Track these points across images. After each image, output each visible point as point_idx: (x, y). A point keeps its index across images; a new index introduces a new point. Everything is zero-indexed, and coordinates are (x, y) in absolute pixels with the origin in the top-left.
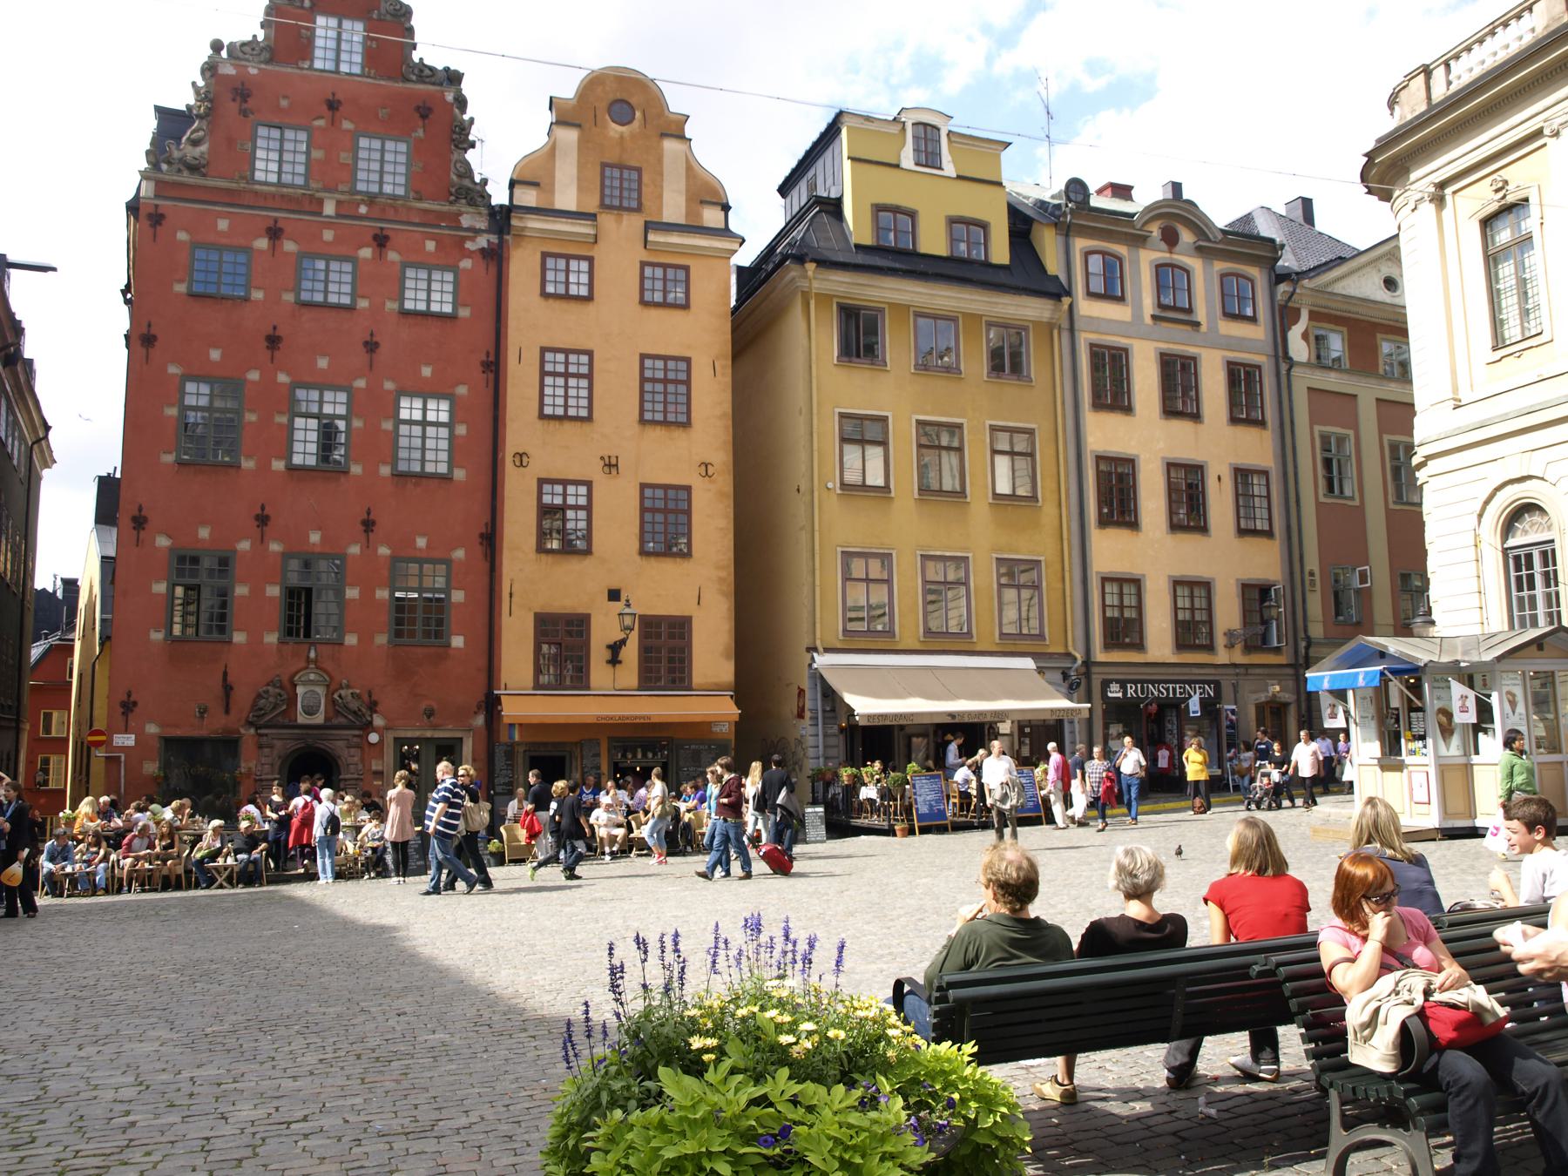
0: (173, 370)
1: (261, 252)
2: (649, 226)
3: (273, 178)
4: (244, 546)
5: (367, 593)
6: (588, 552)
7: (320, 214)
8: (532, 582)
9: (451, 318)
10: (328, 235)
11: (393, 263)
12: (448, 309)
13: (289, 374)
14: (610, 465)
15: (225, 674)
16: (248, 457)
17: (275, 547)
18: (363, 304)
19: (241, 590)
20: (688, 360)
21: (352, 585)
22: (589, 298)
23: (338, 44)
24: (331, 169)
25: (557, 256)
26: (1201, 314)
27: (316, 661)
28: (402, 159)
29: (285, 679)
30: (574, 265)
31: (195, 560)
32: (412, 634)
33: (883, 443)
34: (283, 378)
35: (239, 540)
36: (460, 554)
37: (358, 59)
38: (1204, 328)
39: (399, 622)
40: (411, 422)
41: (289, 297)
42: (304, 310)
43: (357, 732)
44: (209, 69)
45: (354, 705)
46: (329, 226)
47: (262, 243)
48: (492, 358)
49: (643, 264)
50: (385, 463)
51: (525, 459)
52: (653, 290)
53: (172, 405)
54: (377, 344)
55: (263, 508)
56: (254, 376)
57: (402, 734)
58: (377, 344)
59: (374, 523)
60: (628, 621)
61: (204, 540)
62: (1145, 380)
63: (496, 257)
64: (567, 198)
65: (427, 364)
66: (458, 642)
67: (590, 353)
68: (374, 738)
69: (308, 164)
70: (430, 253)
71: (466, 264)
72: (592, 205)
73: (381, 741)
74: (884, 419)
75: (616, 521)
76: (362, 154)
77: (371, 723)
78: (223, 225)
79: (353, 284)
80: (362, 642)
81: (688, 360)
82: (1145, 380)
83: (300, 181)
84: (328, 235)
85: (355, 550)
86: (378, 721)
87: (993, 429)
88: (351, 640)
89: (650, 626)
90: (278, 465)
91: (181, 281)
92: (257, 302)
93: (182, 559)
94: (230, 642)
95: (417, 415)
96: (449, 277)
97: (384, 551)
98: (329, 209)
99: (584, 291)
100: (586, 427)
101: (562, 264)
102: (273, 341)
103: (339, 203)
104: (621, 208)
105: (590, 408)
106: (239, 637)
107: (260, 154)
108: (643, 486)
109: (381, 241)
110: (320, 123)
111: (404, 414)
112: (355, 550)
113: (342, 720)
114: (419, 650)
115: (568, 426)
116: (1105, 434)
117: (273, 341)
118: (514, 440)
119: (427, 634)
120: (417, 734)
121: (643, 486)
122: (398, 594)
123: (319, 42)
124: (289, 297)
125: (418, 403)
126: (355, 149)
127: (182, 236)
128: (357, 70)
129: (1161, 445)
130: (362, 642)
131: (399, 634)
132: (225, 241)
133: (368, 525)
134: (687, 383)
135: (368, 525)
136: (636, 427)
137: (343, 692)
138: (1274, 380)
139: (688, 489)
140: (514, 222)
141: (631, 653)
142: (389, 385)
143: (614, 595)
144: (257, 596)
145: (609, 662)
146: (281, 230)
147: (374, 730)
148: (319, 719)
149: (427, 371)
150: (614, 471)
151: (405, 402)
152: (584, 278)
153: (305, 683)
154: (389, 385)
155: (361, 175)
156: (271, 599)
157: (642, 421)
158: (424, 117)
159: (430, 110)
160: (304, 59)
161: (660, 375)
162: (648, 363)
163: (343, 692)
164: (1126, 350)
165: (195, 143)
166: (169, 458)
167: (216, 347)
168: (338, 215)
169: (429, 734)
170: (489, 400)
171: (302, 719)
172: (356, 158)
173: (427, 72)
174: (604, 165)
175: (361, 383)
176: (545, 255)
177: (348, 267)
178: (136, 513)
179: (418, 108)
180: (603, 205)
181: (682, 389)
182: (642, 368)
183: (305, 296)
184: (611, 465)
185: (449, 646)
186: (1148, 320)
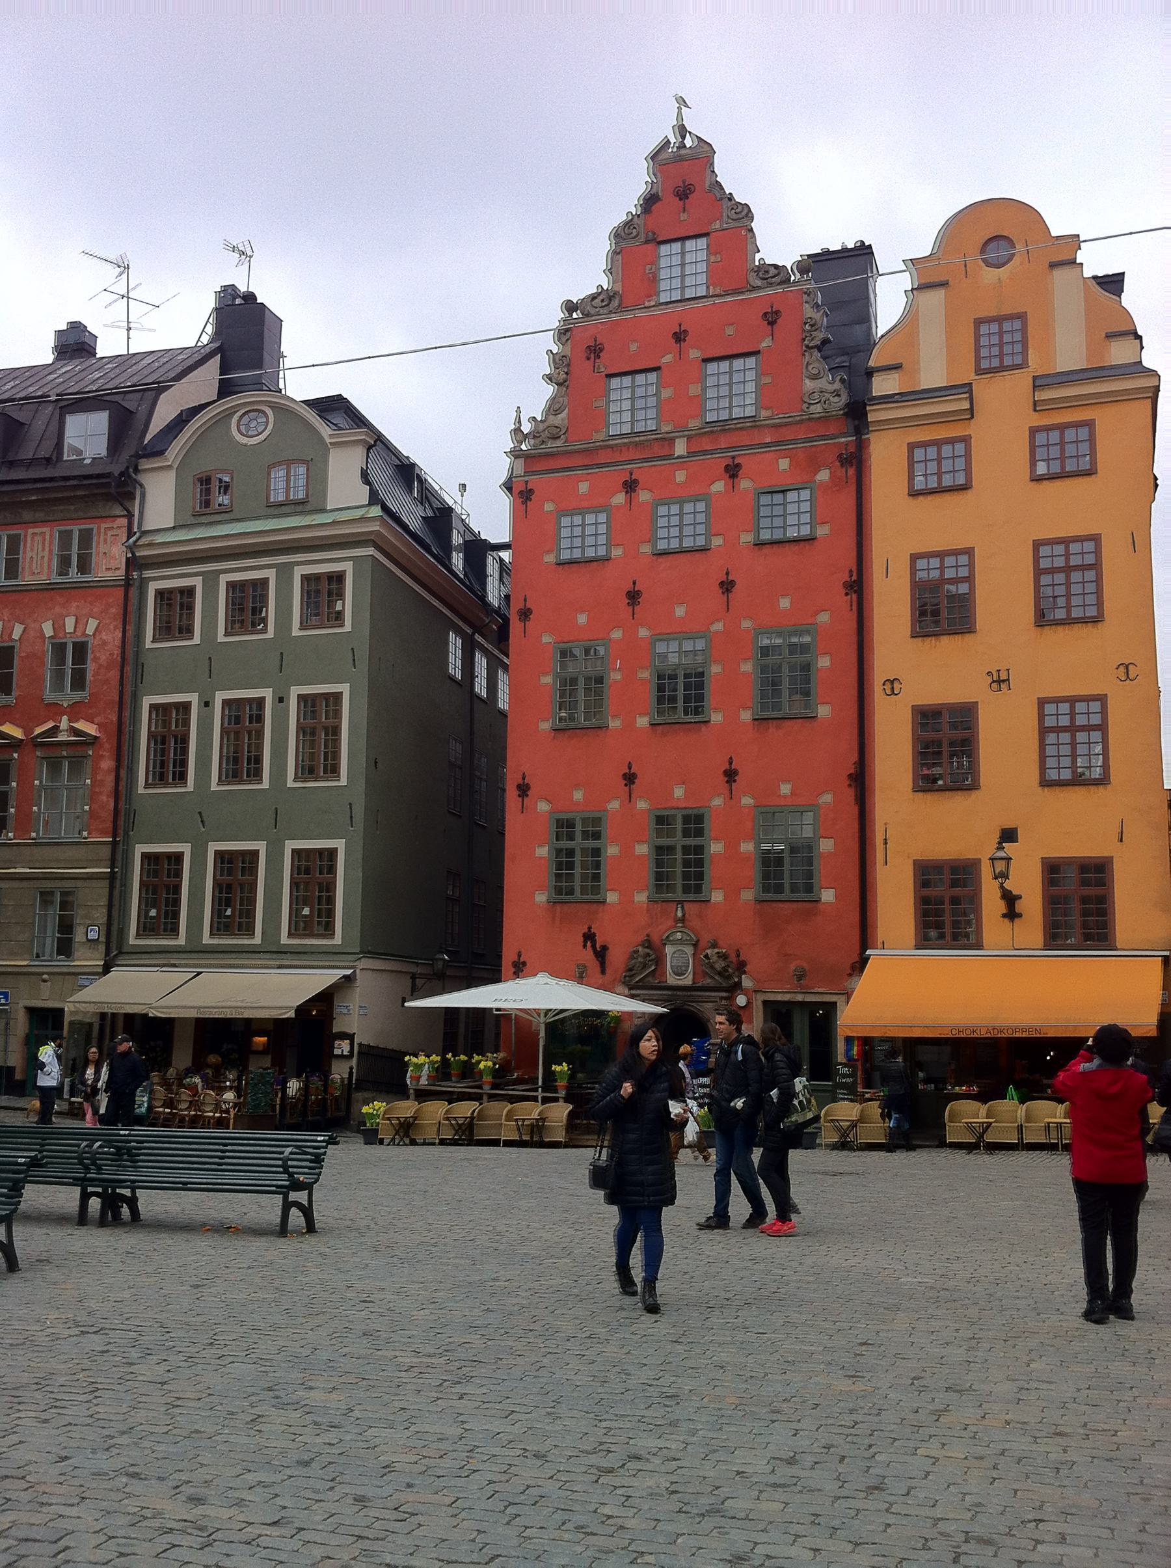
0: (546, 639)
1: (618, 508)
2: (1039, 383)
3: (626, 429)
5: (733, 846)
8: (912, 826)
9: (810, 539)
10: (680, 476)
12: (805, 531)
13: (649, 628)
14: (999, 682)
15: (589, 937)
16: (615, 716)
17: (642, 805)
18: (717, 542)
19: (612, 850)
20: (1096, 539)
21: (717, 839)
22: (965, 488)
23: (684, 269)
27: (683, 920)
28: (751, 375)
29: (655, 938)
30: (947, 450)
31: (570, 824)
32: (779, 889)
34: (643, 632)
35: (609, 801)
36: (827, 798)
37: (702, 279)
39: (766, 876)
41: (646, 549)
43: (724, 994)
44: (564, 333)
45: (720, 965)
47: (620, 499)
48: (854, 578)
49: (1033, 431)
50: (745, 708)
51: (896, 684)
52: (1048, 460)
53: (546, 674)
54: (732, 583)
55: (630, 768)
57: (772, 997)
58: (732, 583)
59: (736, 772)
60: (1000, 866)
61: (578, 803)
63: (855, 461)
64: (932, 375)
66: (828, 896)
67: (969, 552)
68: (741, 1000)
69: (659, 406)
71: (824, 475)
72: (967, 374)
73: (749, 1003)
76: (711, 381)
77: (740, 983)
78: (583, 487)
79: (706, 523)
80: (731, 896)
81: (1096, 539)
83: (652, 425)
85: (718, 802)
86: (747, 982)
88: (717, 896)
89: (1052, 869)
90: (643, 722)
91: (548, 552)
93: (560, 823)
94: (604, 902)
97: (747, 801)
98: (680, 448)
101: (932, 452)
102: (633, 596)
103: (689, 438)
104: (1001, 369)
106: (612, 898)
107: (614, 407)
108: (1042, 702)
109: (733, 471)
110: (668, 358)
112: (718, 802)
113: (708, 981)
114: (787, 905)
117: (633, 596)
118: (882, 667)
119: (794, 888)
120: (787, 997)
121: (1042, 702)
122: (765, 847)
123: (663, 274)
124: (646, 549)
126: (702, 379)
127: (549, 507)
128: (702, 291)
130: (731, 896)
131: (766, 889)
132: (585, 504)
133: (731, 775)
135: (731, 775)
137: (709, 951)
139: (1102, 699)
140: (871, 418)
141: (1032, 903)
142: (746, 624)
143: (1009, 835)
144: (628, 853)
145: (1004, 916)
146: (636, 481)
147: (745, 992)
148: (687, 980)
149: (785, 603)
152: (960, 464)
153: (673, 943)
154: (746, 624)
155: (711, 405)
156: (640, 857)
158: (772, 323)
159: (777, 312)
161: (1060, 562)
162: (1044, 551)
163: (709, 951)
166: (546, 726)
168: (691, 454)
169: (800, 998)
170: (854, 625)
171: (672, 980)
172: (704, 389)
173: (773, 271)
174: (978, 322)
175: (718, 627)
176: (912, 447)
178: (521, 782)
179: (766, 314)
180: (980, 371)
181: (1090, 575)
183: (662, 545)
184: (1000, 681)
185: (818, 901)
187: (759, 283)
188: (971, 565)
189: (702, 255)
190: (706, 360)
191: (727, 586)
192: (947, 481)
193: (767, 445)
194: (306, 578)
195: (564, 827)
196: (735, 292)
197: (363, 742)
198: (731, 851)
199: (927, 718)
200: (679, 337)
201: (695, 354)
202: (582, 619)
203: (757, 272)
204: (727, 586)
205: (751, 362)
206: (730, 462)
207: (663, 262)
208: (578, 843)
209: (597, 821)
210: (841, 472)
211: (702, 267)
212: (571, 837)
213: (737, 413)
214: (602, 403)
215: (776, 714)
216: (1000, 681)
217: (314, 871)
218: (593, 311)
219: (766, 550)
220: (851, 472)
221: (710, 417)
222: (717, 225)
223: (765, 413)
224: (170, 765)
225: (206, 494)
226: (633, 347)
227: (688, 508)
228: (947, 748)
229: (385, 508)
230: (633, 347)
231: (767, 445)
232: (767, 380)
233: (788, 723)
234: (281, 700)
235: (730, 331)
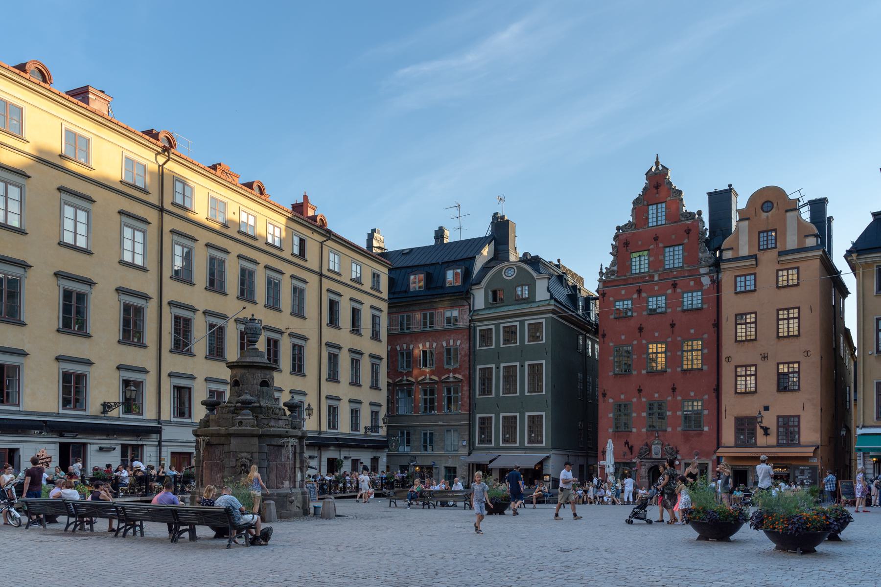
12: (699, 306)
18: (669, 310)
22: (755, 291)
25: (741, 276)
46: (656, 284)
84: (656, 288)
96: (699, 293)
99: (753, 288)
101: (743, 279)
109: (675, 286)
152: (753, 282)
176: (736, 277)
177: (664, 298)
192: (748, 288)
194: (529, 325)
217: (535, 422)
224: (486, 389)
225: (495, 298)
227: (659, 298)
229: (556, 300)
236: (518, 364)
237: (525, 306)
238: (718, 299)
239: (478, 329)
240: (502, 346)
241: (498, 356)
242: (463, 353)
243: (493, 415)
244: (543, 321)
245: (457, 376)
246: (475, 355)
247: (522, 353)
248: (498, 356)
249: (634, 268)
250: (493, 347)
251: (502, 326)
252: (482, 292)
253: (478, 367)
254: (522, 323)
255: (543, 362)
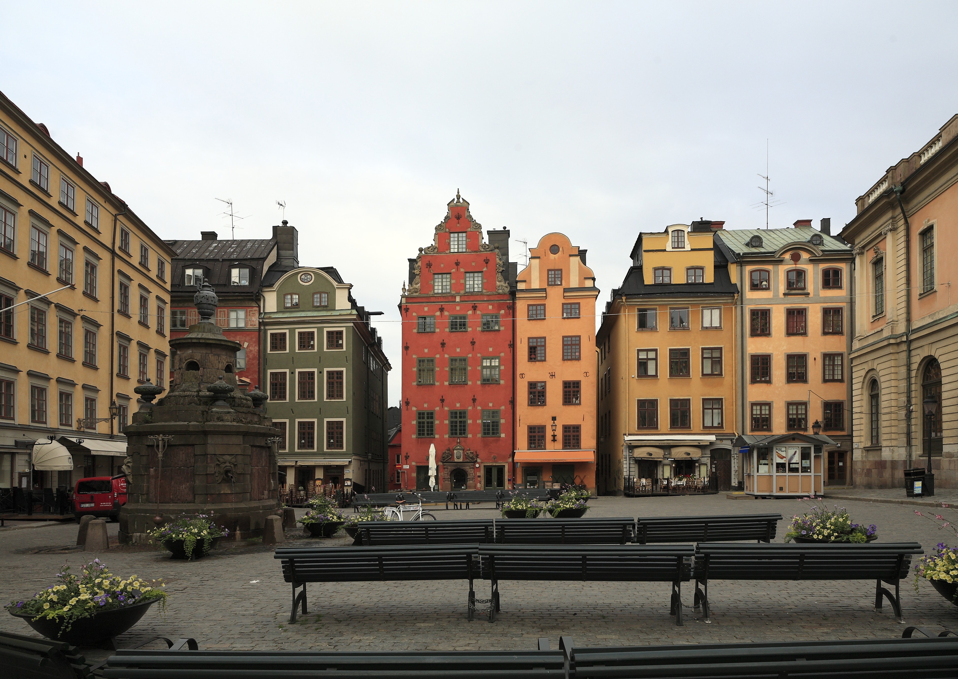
0: (414, 356)
1: (438, 316)
3: (440, 291)
4: (437, 409)
6: (545, 405)
7: (455, 302)
9: (498, 331)
10: (458, 308)
11: (479, 314)
13: (448, 355)
14: (552, 375)
16: (437, 381)
21: (470, 419)
24: (459, 286)
26: (810, 288)
28: (480, 279)
31: (423, 414)
33: (656, 359)
34: (446, 356)
36: (503, 407)
37: (464, 246)
38: (811, 295)
40: (486, 367)
42: (452, 333)
46: (458, 305)
47: (438, 313)
50: (478, 380)
51: (523, 375)
53: (414, 367)
56: (438, 356)
61: (425, 408)
62: (778, 321)
65: (491, 347)
67: (545, 338)
69: (451, 285)
70: (490, 310)
71: (502, 312)
74: (656, 350)
75: (554, 393)
78: (426, 309)
82: (778, 321)
83: (448, 291)
84: (458, 308)
85: (470, 408)
87: (703, 349)
90: (446, 383)
91: (415, 328)
92: (438, 332)
93: (419, 414)
95: (488, 364)
97: (479, 408)
98: (458, 299)
100: (544, 362)
102: (443, 344)
105: (545, 357)
107: (436, 284)
109: (475, 308)
110: (453, 270)
111: (484, 364)
112: (470, 408)
115: (537, 363)
116: (756, 346)
117: (443, 344)
125: (489, 361)
128: (464, 250)
129: (785, 348)
132: (427, 314)
133: (474, 400)
134: (579, 345)
135: (474, 400)
136: (562, 362)
138: (849, 313)
142: (479, 355)
146: (443, 308)
149: (491, 349)
150: (553, 377)
151: (485, 361)
154: (479, 355)
157: (564, 360)
158: (487, 263)
159: (488, 260)
160: (447, 250)
161: (569, 343)
164: (769, 310)
165: (416, 284)
166: (415, 384)
167: (426, 348)
168: (461, 301)
170: (511, 357)
172: (465, 281)
175: (470, 355)
182: (563, 341)
186: (781, 296)
187: (483, 250)
188: (545, 342)
189: (464, 239)
190: (466, 272)
191: (473, 343)
193: (485, 301)
195: (421, 415)
196: (475, 252)
197: (351, 387)
198: (474, 423)
199: (532, 385)
200: (457, 264)
201: (462, 270)
202: (426, 351)
203: (482, 246)
204: (473, 343)
205: (480, 274)
206: (473, 305)
207: (452, 239)
208: (426, 420)
209: (432, 414)
210: (508, 311)
211: (464, 242)
212: (423, 418)
213: (476, 290)
214: (432, 282)
215: (488, 383)
216: (552, 376)
218: (428, 252)
219: (485, 333)
220: (511, 311)
221: (468, 290)
222: (469, 229)
223: (484, 291)
226: (442, 265)
228: (537, 395)
230: (442, 265)
231: (485, 301)
232: (485, 281)
233: (491, 385)
234: (320, 372)
235: (473, 264)
236: (315, 370)
237: (324, 313)
238: (514, 323)
239: (269, 332)
240: (297, 351)
241: (292, 361)
242: (251, 356)
243: (287, 421)
244: (344, 329)
245: (243, 379)
246: (265, 360)
247: (320, 360)
248: (292, 361)
249: (436, 288)
250: (287, 351)
251: (297, 331)
252: (275, 294)
253: (269, 371)
254: (320, 330)
255: (344, 369)
